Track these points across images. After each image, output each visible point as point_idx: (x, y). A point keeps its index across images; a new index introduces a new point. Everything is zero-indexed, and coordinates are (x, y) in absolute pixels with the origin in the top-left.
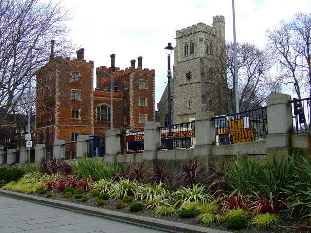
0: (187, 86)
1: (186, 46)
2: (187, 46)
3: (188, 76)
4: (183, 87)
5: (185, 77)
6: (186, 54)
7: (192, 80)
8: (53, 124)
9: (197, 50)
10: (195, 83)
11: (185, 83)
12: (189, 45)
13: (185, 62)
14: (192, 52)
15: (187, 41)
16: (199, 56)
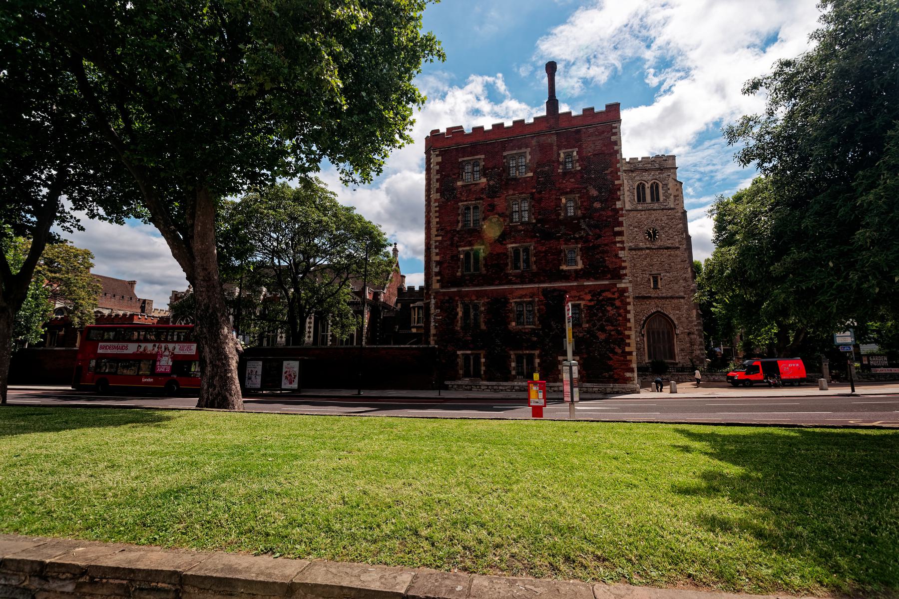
0: (648, 251)
1: (641, 188)
2: (644, 188)
3: (652, 235)
4: (639, 253)
5: (641, 237)
6: (641, 198)
7: (659, 243)
8: (597, 279)
9: (667, 197)
10: (668, 248)
11: (641, 245)
12: (647, 186)
13: (643, 213)
14: (655, 197)
15: (644, 178)
16: (672, 206)
